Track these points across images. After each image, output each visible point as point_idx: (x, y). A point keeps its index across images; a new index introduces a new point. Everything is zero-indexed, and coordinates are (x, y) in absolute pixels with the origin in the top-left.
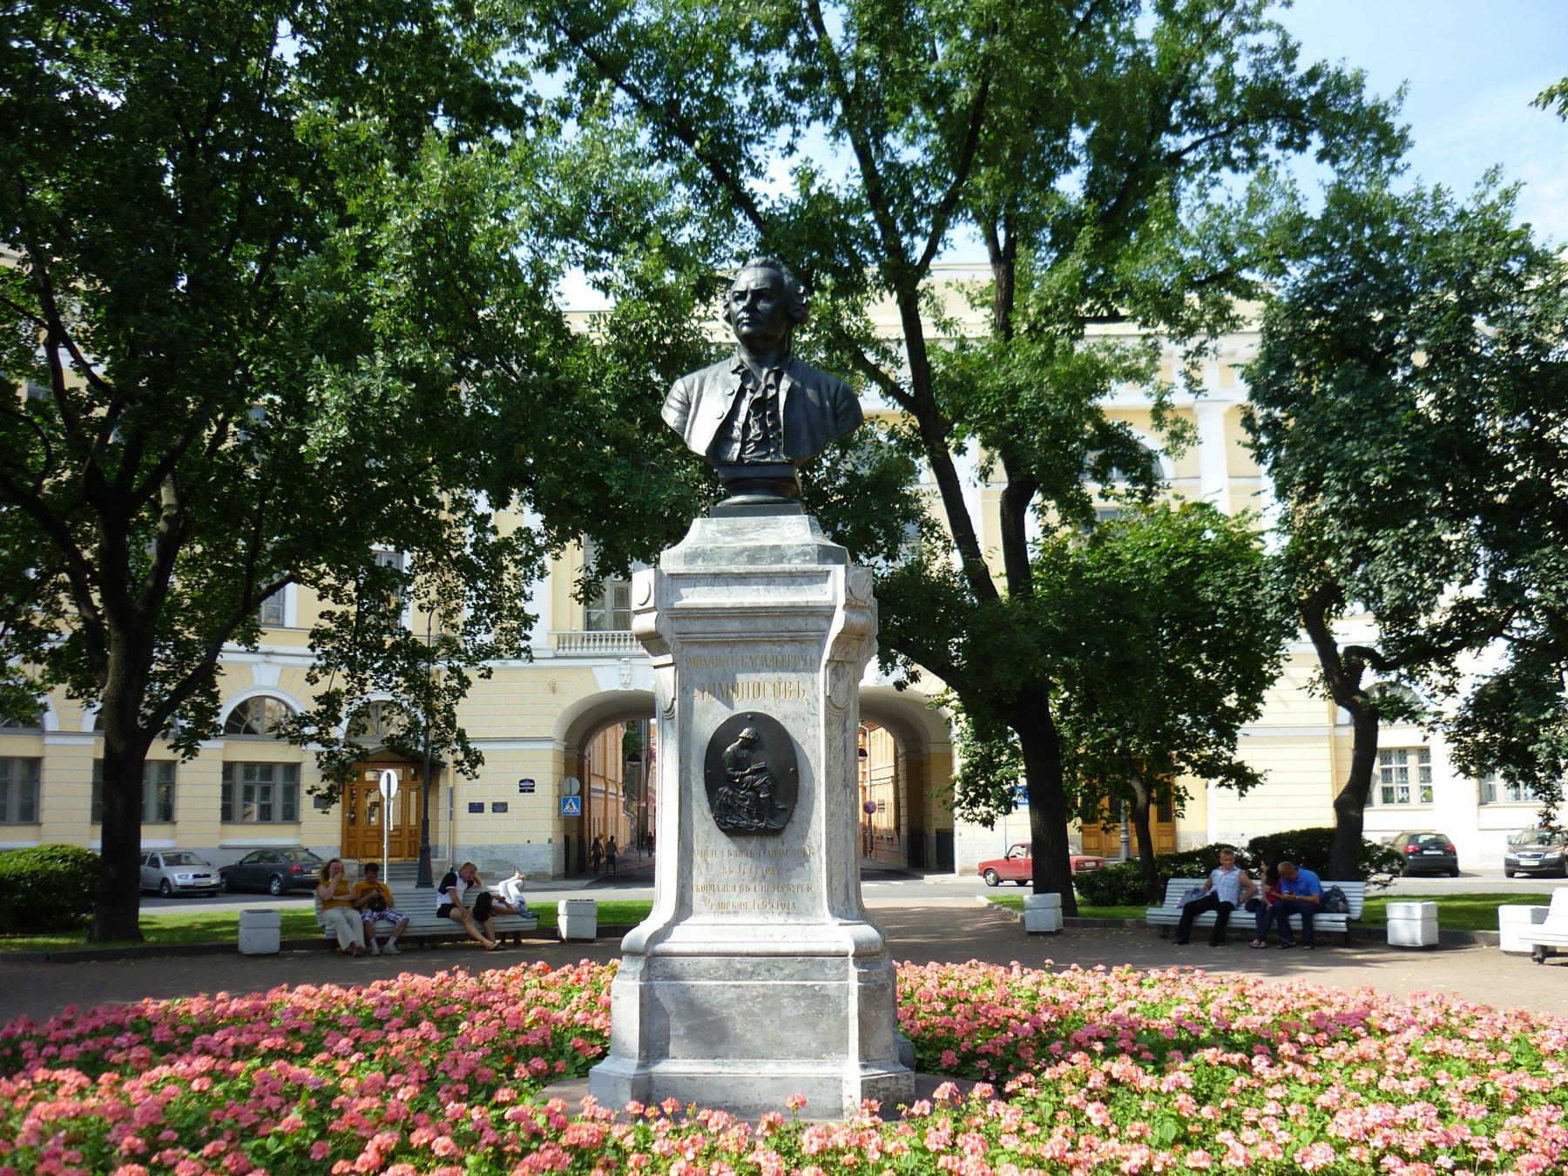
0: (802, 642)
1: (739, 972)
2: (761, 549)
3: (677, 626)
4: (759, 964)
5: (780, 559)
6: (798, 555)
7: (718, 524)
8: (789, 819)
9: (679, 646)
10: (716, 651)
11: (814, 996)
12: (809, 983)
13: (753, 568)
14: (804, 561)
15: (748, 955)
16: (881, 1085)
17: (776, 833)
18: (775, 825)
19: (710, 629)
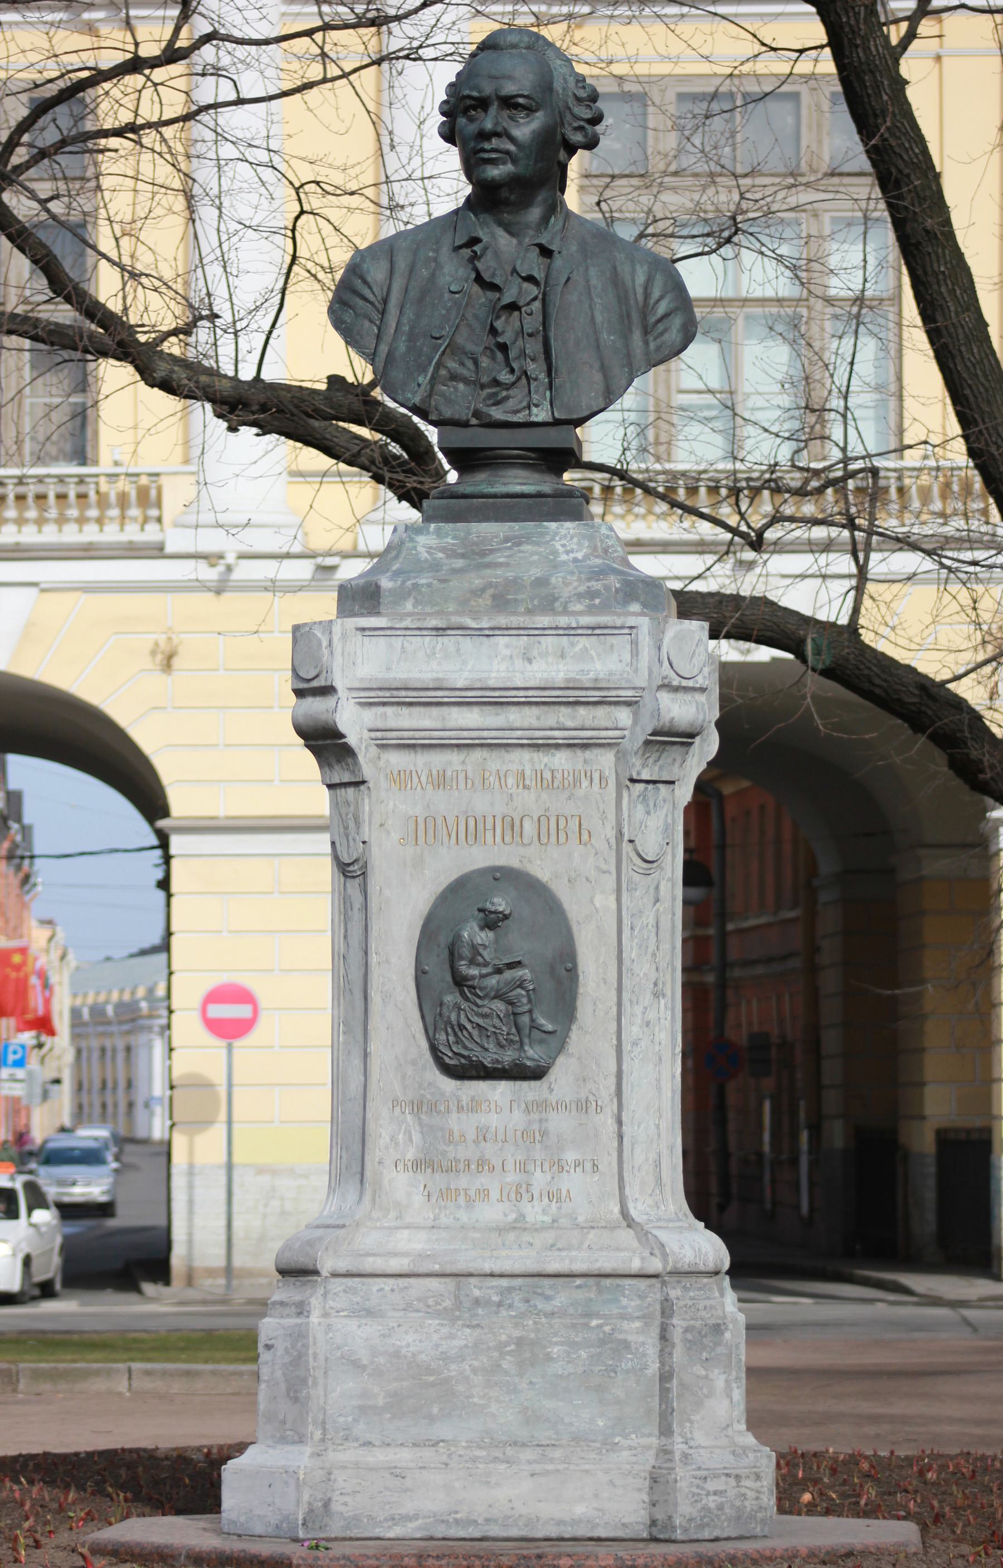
0: (585, 746)
1: (477, 1302)
2: (515, 584)
3: (370, 717)
4: (510, 1290)
5: (549, 604)
6: (580, 596)
7: (438, 533)
8: (561, 1048)
9: (374, 751)
10: (438, 759)
11: (602, 1342)
12: (594, 1323)
13: (502, 621)
14: (591, 610)
15: (492, 1275)
16: (711, 1486)
17: (537, 1074)
18: (533, 1054)
19: (427, 723)
